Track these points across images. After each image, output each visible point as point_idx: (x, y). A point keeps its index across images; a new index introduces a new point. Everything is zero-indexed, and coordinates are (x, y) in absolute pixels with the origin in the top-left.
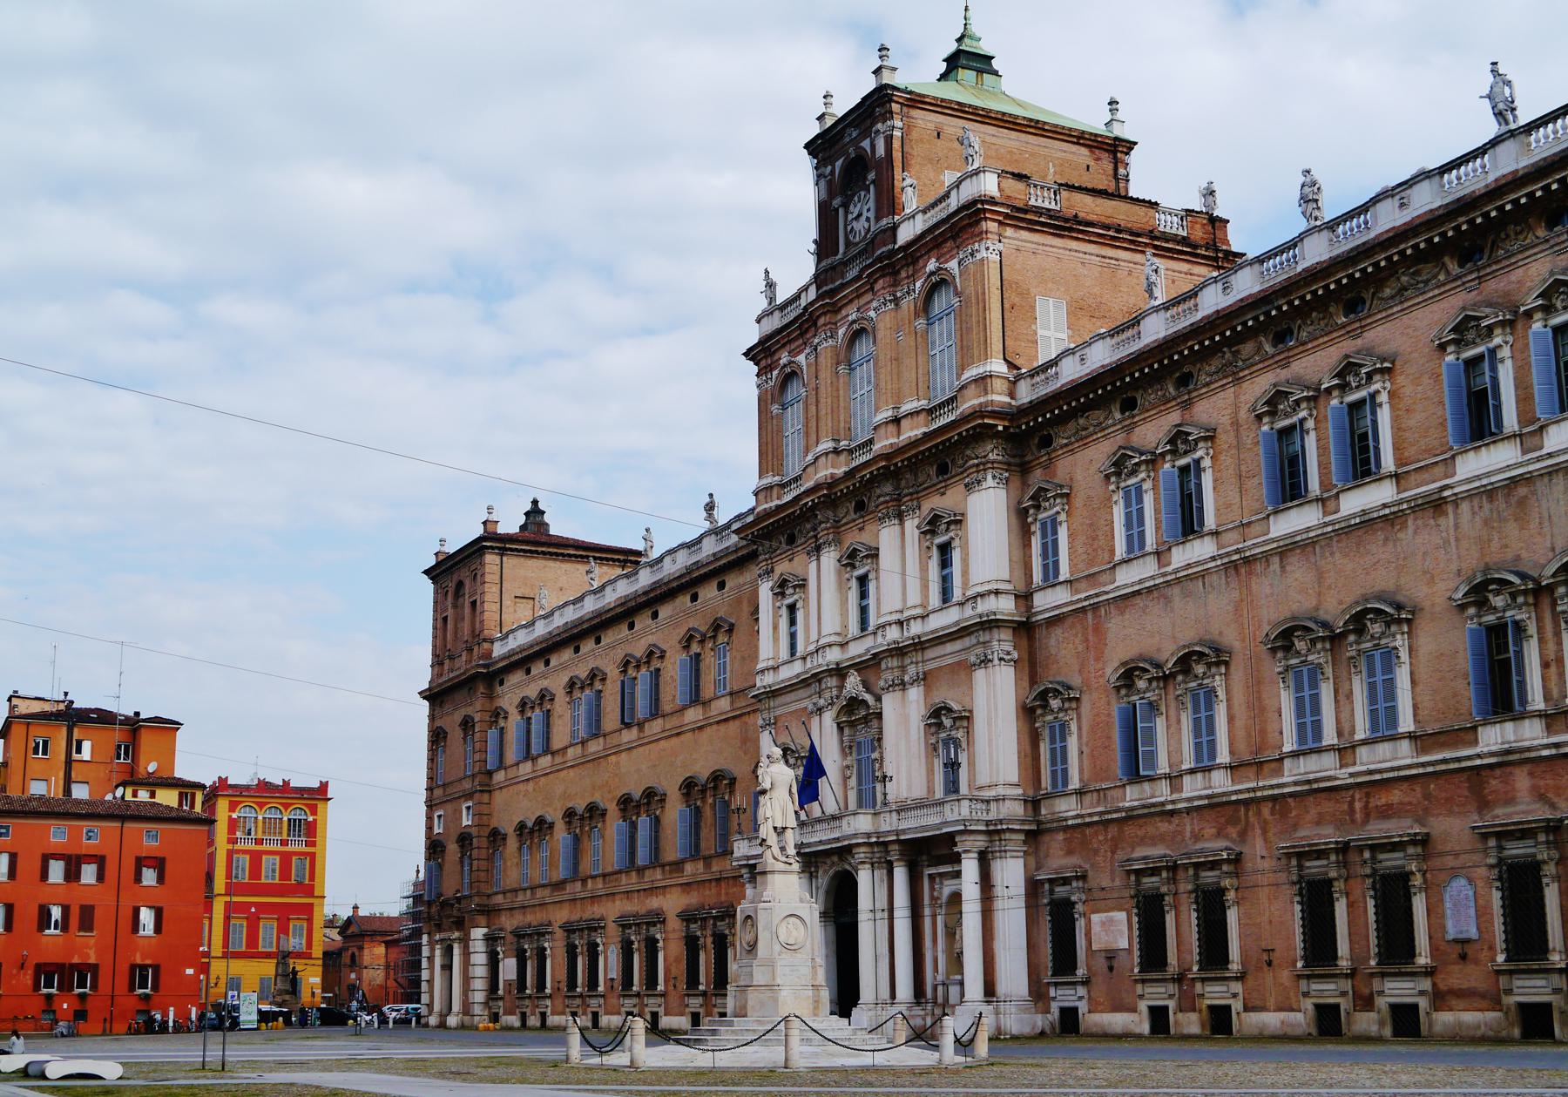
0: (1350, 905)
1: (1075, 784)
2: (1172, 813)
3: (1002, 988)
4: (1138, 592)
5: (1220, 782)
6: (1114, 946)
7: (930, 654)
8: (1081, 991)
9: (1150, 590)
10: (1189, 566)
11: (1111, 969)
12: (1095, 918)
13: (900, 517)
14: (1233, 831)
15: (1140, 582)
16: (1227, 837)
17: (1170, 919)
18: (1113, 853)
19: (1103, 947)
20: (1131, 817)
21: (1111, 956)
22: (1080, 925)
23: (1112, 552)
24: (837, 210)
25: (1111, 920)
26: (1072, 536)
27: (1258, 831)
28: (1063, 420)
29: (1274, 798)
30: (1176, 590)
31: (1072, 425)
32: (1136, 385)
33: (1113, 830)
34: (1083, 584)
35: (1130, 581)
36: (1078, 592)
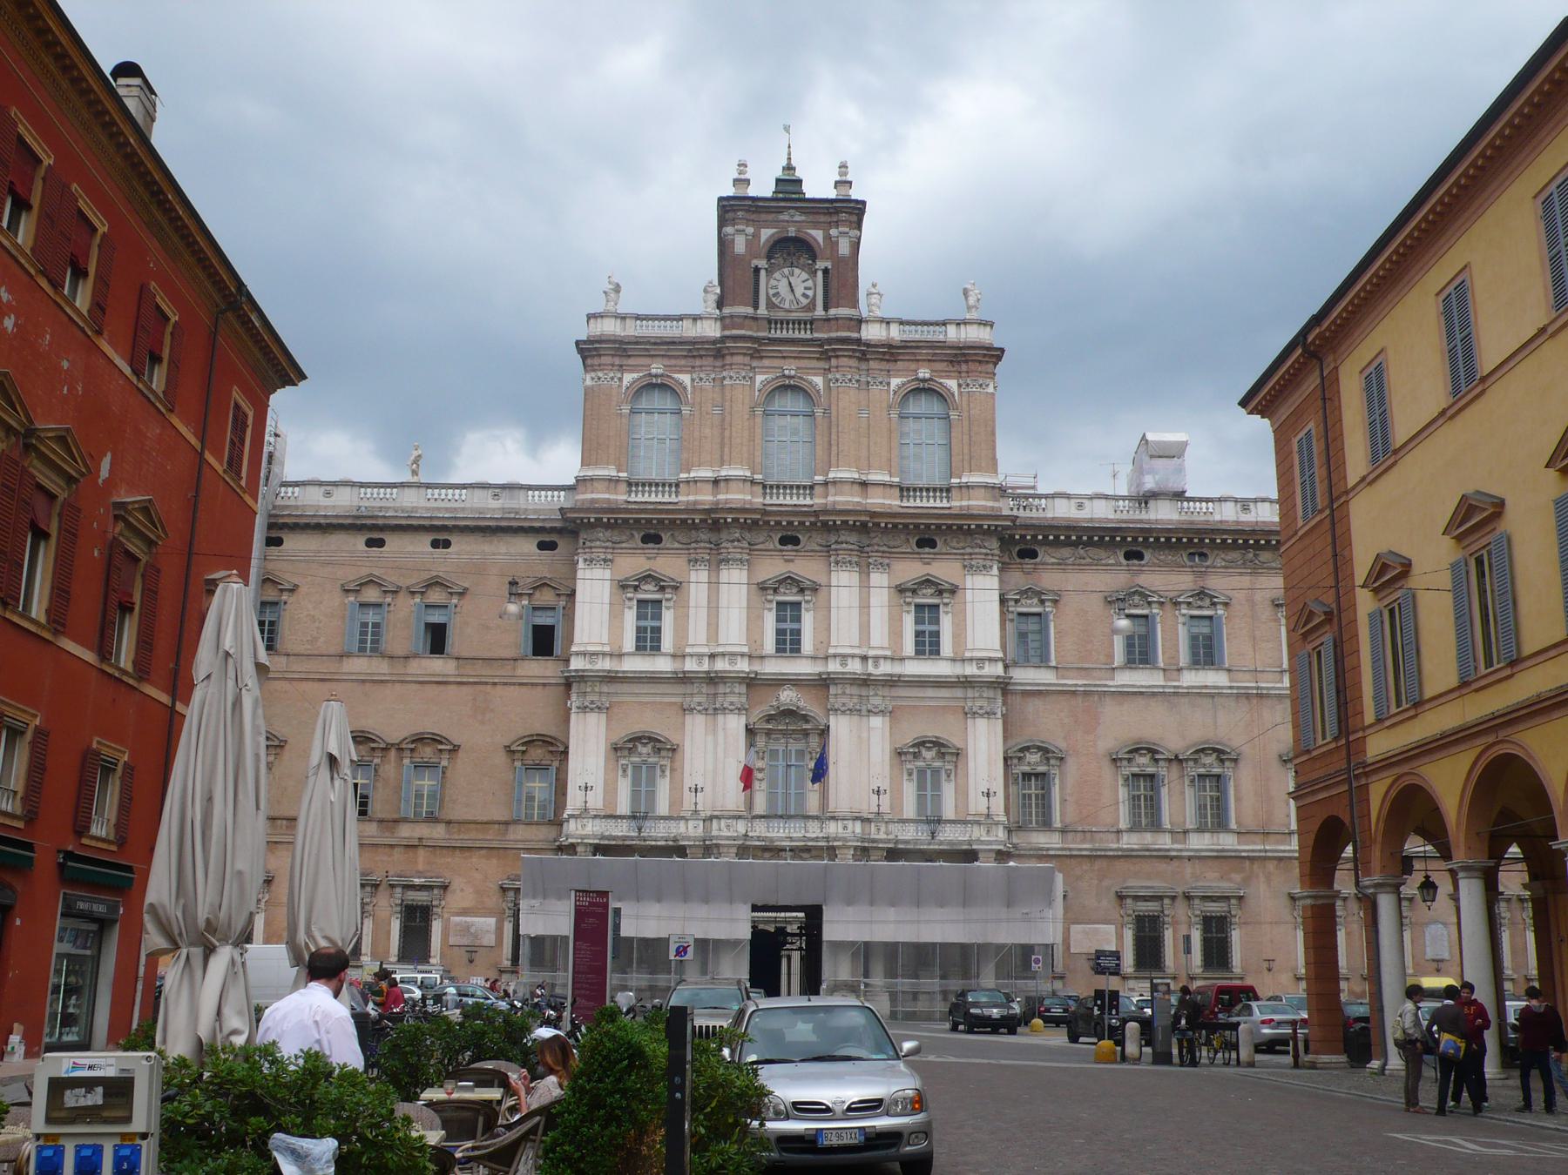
0: (1348, 934)
2: (1172, 858)
4: (1142, 693)
5: (1228, 842)
9: (1154, 694)
13: (865, 570)
14: (1237, 877)
16: (1230, 880)
17: (1168, 935)
20: (1128, 856)
23: (1111, 657)
24: (757, 270)
27: (1262, 879)
28: (1057, 543)
29: (1280, 859)
30: (1185, 700)
33: (1098, 864)
36: (1063, 677)
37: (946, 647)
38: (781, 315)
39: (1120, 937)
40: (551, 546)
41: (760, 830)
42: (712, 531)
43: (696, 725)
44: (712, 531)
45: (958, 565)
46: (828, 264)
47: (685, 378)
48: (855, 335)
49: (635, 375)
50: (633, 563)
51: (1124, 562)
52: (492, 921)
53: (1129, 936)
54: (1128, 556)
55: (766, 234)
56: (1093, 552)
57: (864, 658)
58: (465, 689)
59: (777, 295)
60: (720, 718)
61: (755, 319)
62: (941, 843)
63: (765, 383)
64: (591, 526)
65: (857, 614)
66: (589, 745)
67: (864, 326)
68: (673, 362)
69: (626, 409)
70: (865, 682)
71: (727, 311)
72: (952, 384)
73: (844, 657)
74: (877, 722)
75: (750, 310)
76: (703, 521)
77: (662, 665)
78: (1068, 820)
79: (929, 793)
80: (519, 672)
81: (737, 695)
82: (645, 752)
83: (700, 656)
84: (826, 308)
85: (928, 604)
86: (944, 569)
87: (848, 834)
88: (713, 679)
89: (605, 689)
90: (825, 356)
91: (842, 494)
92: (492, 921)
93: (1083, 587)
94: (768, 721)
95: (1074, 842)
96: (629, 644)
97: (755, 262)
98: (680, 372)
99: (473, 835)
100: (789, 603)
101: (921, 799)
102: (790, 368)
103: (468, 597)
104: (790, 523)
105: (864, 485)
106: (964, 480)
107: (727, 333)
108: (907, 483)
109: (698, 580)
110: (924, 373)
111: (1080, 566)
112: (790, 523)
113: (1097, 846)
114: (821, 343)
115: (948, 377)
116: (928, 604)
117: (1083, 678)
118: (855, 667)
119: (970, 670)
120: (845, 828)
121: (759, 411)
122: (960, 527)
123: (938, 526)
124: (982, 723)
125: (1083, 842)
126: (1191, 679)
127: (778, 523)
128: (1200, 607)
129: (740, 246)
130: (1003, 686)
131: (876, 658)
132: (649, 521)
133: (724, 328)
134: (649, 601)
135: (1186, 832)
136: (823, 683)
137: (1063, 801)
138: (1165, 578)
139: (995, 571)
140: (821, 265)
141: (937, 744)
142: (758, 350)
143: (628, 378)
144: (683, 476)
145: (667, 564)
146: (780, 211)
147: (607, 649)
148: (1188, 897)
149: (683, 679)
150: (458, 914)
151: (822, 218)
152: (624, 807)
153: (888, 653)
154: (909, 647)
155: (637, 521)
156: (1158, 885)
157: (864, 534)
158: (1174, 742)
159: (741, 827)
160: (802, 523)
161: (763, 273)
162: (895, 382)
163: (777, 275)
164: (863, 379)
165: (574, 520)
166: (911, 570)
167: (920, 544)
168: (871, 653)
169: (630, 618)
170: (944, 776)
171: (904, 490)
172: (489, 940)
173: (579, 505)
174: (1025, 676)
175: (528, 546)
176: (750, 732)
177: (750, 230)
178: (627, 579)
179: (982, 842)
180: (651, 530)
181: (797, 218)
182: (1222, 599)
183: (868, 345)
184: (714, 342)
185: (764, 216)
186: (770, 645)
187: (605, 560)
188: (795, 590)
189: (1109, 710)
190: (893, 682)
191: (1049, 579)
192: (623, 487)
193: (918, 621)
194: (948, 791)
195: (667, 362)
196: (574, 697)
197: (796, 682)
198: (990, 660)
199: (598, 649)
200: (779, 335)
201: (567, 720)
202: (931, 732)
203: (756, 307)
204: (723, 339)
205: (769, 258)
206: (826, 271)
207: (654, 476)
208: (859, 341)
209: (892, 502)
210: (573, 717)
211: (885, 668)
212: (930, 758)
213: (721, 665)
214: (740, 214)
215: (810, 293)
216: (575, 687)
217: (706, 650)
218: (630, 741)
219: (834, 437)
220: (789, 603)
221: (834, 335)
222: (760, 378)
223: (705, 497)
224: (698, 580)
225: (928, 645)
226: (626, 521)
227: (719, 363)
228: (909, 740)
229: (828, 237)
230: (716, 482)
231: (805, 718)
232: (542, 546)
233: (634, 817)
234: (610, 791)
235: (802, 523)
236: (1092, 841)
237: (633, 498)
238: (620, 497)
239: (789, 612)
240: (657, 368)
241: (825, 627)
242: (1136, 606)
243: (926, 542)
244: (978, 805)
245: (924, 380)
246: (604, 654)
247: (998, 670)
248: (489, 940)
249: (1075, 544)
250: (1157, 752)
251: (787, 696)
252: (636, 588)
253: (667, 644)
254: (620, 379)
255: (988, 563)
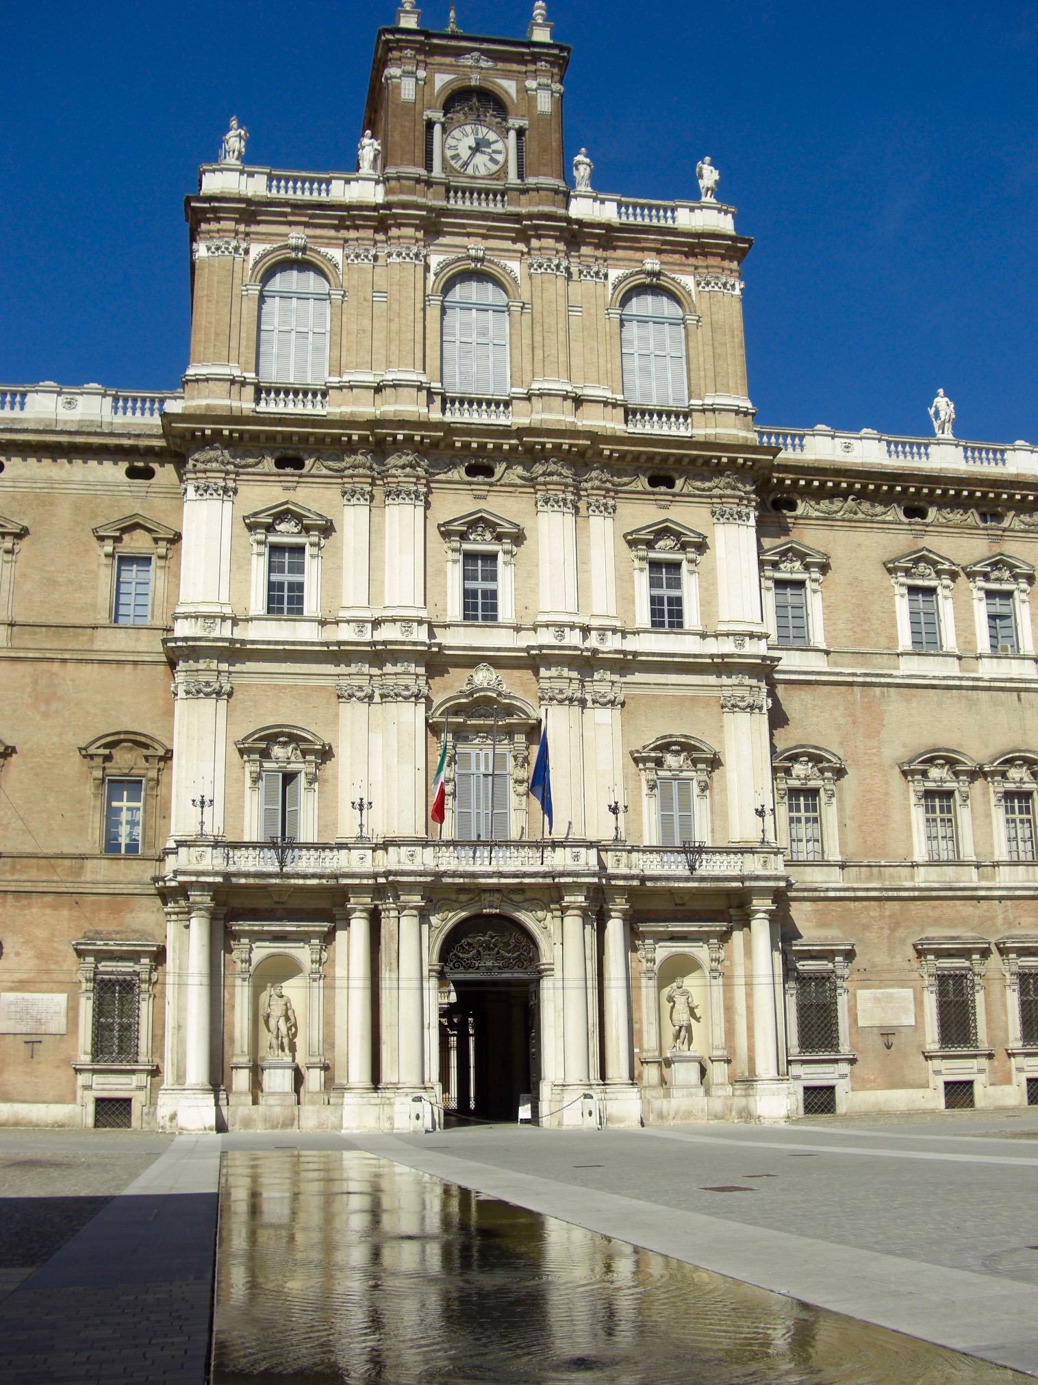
1: (834, 855)
2: (980, 899)
3: (611, 1072)
4: (933, 687)
6: (895, 1023)
7: (638, 677)
8: (844, 1068)
10: (1011, 680)
11: (889, 1047)
12: (864, 995)
15: (945, 678)
17: (979, 998)
18: (893, 930)
19: (877, 1023)
20: (926, 896)
21: (888, 1035)
22: (842, 1001)
23: (893, 639)
24: (430, 125)
25: (891, 996)
26: (828, 608)
28: (820, 494)
31: (825, 504)
32: (932, 500)
34: (847, 659)
35: (931, 674)
36: (836, 664)
37: (692, 618)
38: (464, 182)
39: (919, 1003)
40: (148, 474)
41: (449, 861)
42: (377, 451)
43: (352, 714)
44: (377, 451)
45: (705, 511)
46: (524, 123)
47: (336, 254)
48: (561, 211)
49: (268, 247)
50: (264, 491)
51: (906, 520)
52: (61, 998)
53: (931, 1001)
54: (909, 513)
55: (441, 80)
56: (866, 506)
57: (586, 630)
58: (21, 667)
59: (456, 157)
60: (391, 707)
61: (429, 184)
62: (703, 879)
63: (444, 266)
64: (206, 442)
65: (571, 568)
66: (202, 749)
67: (573, 202)
68: (318, 232)
69: (255, 291)
70: (587, 664)
71: (391, 171)
72: (688, 281)
73: (560, 626)
74: (604, 716)
75: (422, 172)
76: (363, 439)
77: (304, 632)
78: (851, 848)
79: (676, 813)
80: (98, 645)
81: (410, 675)
82: (284, 756)
83: (361, 622)
84: (521, 176)
85: (666, 560)
86: (689, 515)
87: (579, 866)
88: (379, 655)
89: (224, 666)
90: (523, 236)
91: (550, 411)
92: (61, 998)
93: (858, 546)
94: (456, 714)
95: (858, 879)
96: (258, 603)
97: (428, 114)
98: (328, 245)
99: (33, 874)
100: (480, 550)
101: (666, 821)
102: (476, 246)
103: (26, 541)
104: (483, 446)
105: (578, 401)
106: (708, 401)
107: (393, 198)
108: (636, 400)
109: (353, 520)
110: (652, 263)
111: (851, 523)
112: (483, 446)
113: (887, 885)
114: (517, 218)
115: (683, 272)
116: (666, 560)
117: (862, 666)
118: (573, 638)
119: (727, 647)
120: (576, 857)
121: (436, 302)
122: (707, 461)
123: (679, 459)
124: (743, 718)
125: (869, 878)
126: (989, 669)
127: (467, 446)
128: (998, 580)
129: (408, 90)
130: (764, 670)
131: (602, 630)
132: (288, 437)
133: (387, 193)
134: (286, 544)
135: (995, 865)
136: (533, 661)
137: (842, 826)
138: (958, 541)
139: (752, 522)
140: (515, 122)
141: (687, 747)
142: (433, 226)
143: (257, 249)
144: (335, 379)
145: (314, 494)
146: (459, 53)
147: (227, 610)
148: (1003, 951)
149: (338, 655)
150: (12, 989)
151: (515, 67)
152: (252, 830)
153: (618, 624)
154: (643, 617)
155: (272, 437)
156: (966, 934)
157: (585, 464)
158: (976, 752)
159: (426, 859)
160: (498, 447)
161: (437, 129)
162: (614, 274)
163: (456, 133)
164: (574, 270)
165: (182, 435)
166: (642, 513)
167: (654, 482)
168: (595, 623)
169: (259, 566)
170: (695, 789)
171: (630, 413)
172: (58, 1024)
173: (191, 411)
174: (791, 661)
175: (115, 472)
176: (433, 729)
177: (422, 74)
178: (255, 514)
179: (757, 878)
180: (291, 448)
181: (483, 64)
182: (1025, 570)
183: (579, 222)
184: (376, 208)
185: (438, 59)
186: (454, 610)
187: (226, 490)
188: (488, 536)
189: (895, 706)
190: (626, 664)
191: (811, 537)
192: (249, 391)
193: (655, 583)
194: (701, 809)
195: (310, 232)
196: (180, 677)
197: (497, 663)
198: (752, 636)
199: (215, 609)
200: (460, 205)
201: (170, 713)
202: (677, 729)
203: (429, 167)
204: (388, 206)
205: (447, 107)
206: (520, 133)
207: (292, 379)
208: (568, 220)
209: (612, 423)
210: (179, 705)
211: (613, 643)
212: (678, 760)
213: (388, 633)
214: (409, 52)
215: (500, 158)
216: (182, 666)
217: (367, 614)
218: (261, 739)
219: (538, 338)
220: (480, 550)
221: (535, 209)
222: (435, 260)
223: (366, 408)
224: (353, 520)
225: (667, 614)
226: (255, 436)
227: (380, 237)
228: (648, 737)
229: (523, 90)
230: (378, 389)
231: (510, 710)
232: (132, 473)
233: (272, 845)
234: (233, 810)
235: (498, 447)
236: (880, 877)
237: (262, 407)
238: (245, 404)
239: (479, 565)
240: (296, 236)
241: (528, 584)
242: (922, 576)
243: (662, 479)
244: (744, 828)
245: (651, 274)
246: (224, 619)
247: (760, 648)
248: (58, 1024)
249: (844, 495)
250: (957, 762)
251: (483, 677)
252: (270, 528)
253: (311, 605)
254: (247, 252)
255: (744, 510)
